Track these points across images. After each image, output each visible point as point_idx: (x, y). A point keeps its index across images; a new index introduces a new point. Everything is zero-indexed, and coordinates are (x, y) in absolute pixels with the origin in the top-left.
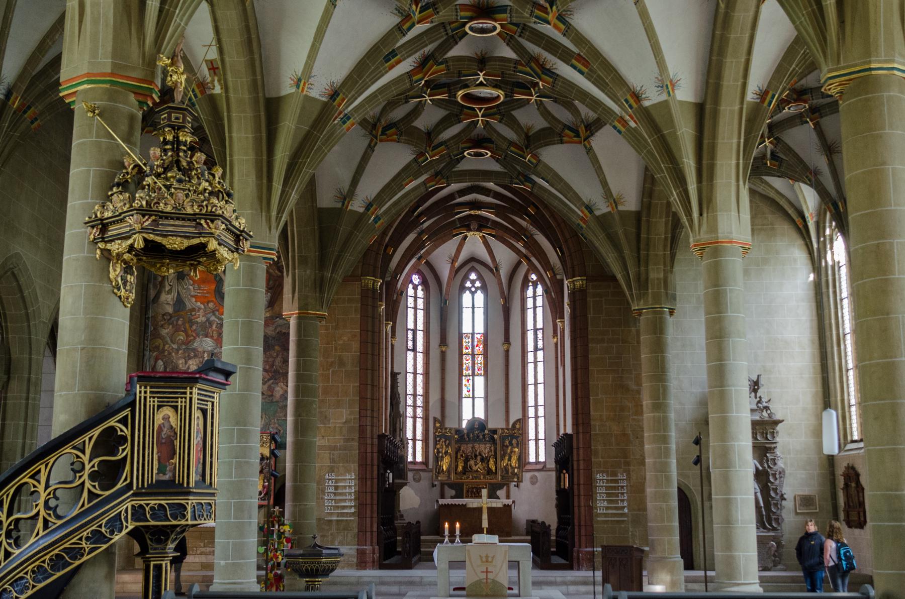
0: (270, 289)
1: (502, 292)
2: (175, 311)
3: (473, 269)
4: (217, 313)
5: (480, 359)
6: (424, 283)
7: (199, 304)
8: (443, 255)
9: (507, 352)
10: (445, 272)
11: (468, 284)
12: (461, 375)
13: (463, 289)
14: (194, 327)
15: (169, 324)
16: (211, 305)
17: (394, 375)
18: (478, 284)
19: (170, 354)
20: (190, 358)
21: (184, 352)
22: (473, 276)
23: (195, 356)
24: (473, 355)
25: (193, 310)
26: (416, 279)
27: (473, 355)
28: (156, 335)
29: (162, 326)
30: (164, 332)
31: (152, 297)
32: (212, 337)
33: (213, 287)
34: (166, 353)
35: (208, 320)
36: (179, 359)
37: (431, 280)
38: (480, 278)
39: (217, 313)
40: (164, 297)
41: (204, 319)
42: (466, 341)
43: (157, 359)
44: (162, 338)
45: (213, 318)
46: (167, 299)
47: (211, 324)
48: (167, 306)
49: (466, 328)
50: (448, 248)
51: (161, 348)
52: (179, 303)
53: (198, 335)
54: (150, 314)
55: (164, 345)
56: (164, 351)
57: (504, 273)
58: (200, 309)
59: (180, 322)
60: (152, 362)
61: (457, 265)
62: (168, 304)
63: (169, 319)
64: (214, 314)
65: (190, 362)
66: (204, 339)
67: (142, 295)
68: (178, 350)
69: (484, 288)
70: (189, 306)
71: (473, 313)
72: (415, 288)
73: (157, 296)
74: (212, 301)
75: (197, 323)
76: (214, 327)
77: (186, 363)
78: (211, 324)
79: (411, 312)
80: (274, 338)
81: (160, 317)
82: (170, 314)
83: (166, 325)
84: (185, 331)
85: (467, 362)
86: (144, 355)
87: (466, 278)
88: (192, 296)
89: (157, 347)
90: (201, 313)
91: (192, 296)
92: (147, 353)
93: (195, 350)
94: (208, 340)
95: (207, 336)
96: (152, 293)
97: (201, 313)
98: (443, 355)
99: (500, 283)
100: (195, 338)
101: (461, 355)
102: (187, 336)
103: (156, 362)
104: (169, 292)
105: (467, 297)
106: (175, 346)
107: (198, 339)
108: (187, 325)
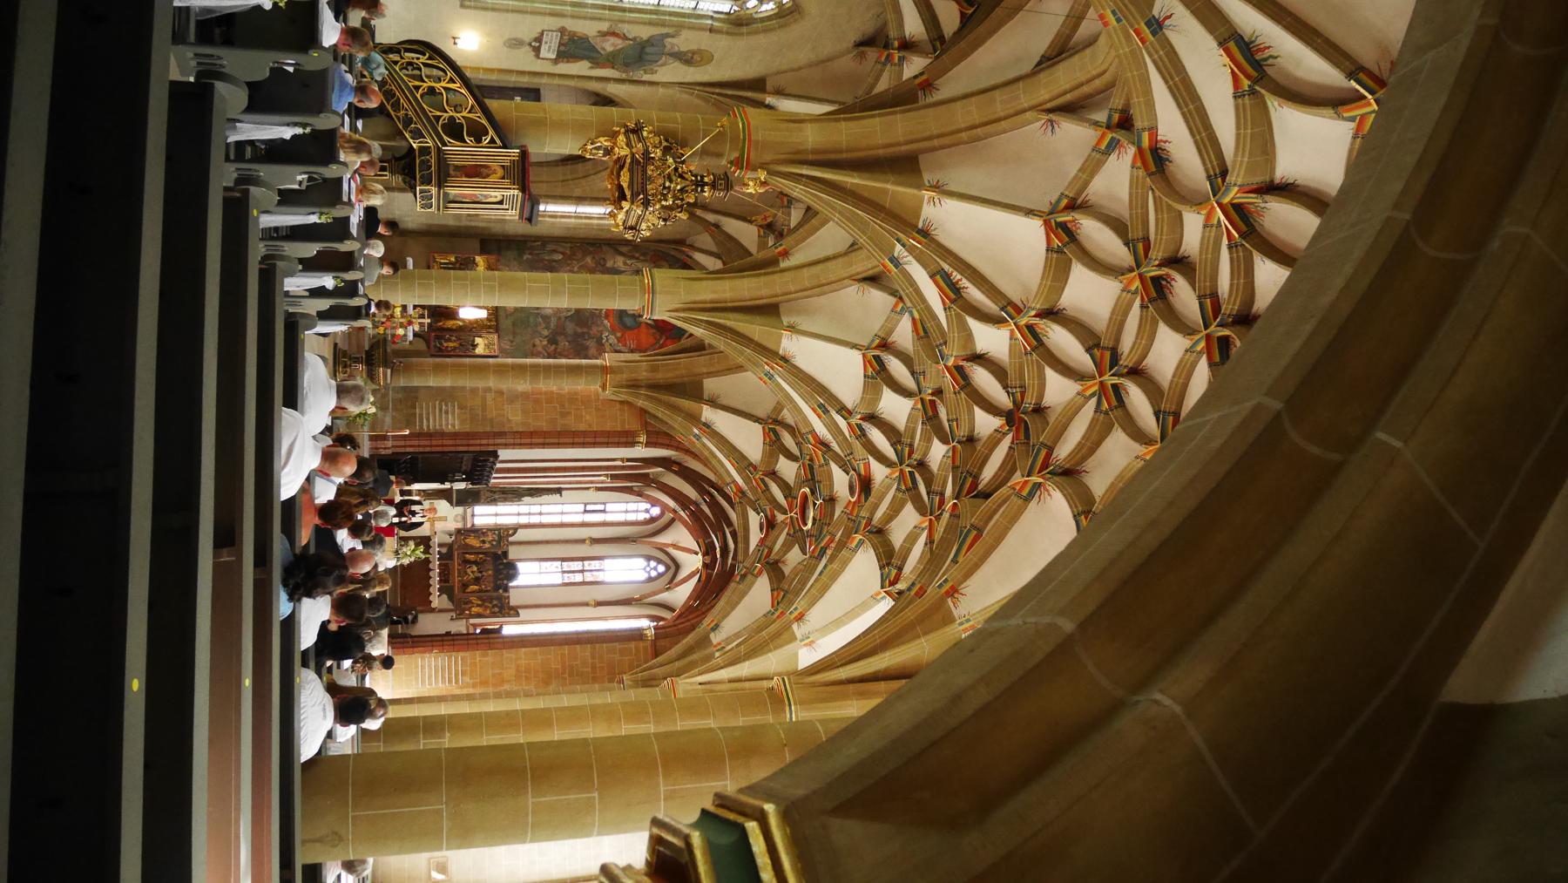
1: (646, 596)
3: (668, 568)
5: (578, 578)
6: (653, 520)
8: (681, 536)
9: (587, 604)
10: (662, 539)
11: (653, 564)
12: (563, 560)
13: (649, 558)
17: (559, 491)
18: (654, 574)
22: (661, 569)
24: (582, 571)
26: (656, 511)
27: (582, 571)
28: (586, 253)
30: (589, 259)
37: (655, 527)
38: (660, 575)
42: (595, 564)
44: (583, 258)
49: (607, 563)
50: (688, 540)
57: (665, 597)
61: (671, 550)
69: (650, 580)
71: (627, 570)
72: (647, 511)
73: (622, 254)
79: (623, 507)
85: (577, 565)
87: (659, 561)
96: (624, 249)
98: (583, 541)
99: (655, 594)
101: (583, 559)
105: (641, 562)
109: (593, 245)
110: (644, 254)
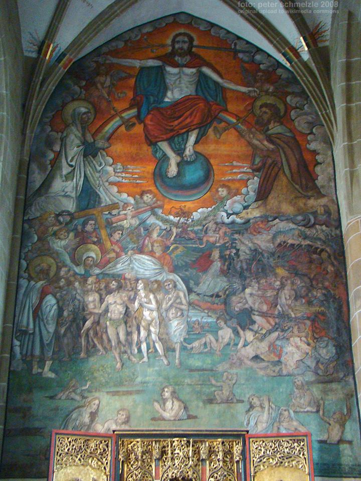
0: (258, 170)
2: (81, 209)
4: (159, 211)
7: (125, 196)
14: (117, 236)
15: (68, 232)
16: (147, 198)
19: (69, 283)
20: (109, 292)
21: (98, 281)
23: (120, 287)
25: (114, 206)
29: (55, 234)
30: (60, 245)
31: (38, 185)
32: (151, 253)
33: (151, 168)
34: (62, 283)
35: (143, 222)
36: (86, 292)
39: (159, 211)
40: (58, 185)
41: (135, 222)
43: (43, 294)
44: (55, 255)
45: (152, 220)
46: (65, 190)
47: (148, 231)
48: (65, 201)
51: (52, 274)
52: (88, 196)
53: (124, 249)
54: (34, 212)
55: (59, 269)
56: (57, 278)
58: (126, 205)
59: (89, 228)
60: (34, 299)
62: (66, 196)
63: (67, 221)
64: (154, 214)
65: (110, 299)
66: (137, 256)
67: (19, 179)
68: (84, 278)
70: (106, 199)
73: (47, 184)
74: (150, 192)
75: (122, 228)
76: (155, 235)
77: (102, 300)
78: (148, 231)
80: (273, 254)
81: (51, 219)
82: (69, 214)
83: (63, 234)
84: (99, 243)
86: (18, 287)
88: (111, 183)
89: (45, 273)
90: (129, 211)
91: (111, 183)
92: (24, 282)
93: (118, 277)
94: (145, 258)
95: (141, 251)
96: (38, 179)
97: (129, 211)
100: (118, 256)
102: (104, 251)
103: (42, 299)
104: (69, 177)
106: (80, 270)
107: (124, 257)
108: (103, 233)
109: (25, 235)
110: (49, 144)
